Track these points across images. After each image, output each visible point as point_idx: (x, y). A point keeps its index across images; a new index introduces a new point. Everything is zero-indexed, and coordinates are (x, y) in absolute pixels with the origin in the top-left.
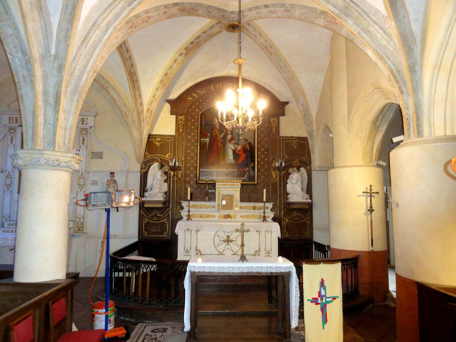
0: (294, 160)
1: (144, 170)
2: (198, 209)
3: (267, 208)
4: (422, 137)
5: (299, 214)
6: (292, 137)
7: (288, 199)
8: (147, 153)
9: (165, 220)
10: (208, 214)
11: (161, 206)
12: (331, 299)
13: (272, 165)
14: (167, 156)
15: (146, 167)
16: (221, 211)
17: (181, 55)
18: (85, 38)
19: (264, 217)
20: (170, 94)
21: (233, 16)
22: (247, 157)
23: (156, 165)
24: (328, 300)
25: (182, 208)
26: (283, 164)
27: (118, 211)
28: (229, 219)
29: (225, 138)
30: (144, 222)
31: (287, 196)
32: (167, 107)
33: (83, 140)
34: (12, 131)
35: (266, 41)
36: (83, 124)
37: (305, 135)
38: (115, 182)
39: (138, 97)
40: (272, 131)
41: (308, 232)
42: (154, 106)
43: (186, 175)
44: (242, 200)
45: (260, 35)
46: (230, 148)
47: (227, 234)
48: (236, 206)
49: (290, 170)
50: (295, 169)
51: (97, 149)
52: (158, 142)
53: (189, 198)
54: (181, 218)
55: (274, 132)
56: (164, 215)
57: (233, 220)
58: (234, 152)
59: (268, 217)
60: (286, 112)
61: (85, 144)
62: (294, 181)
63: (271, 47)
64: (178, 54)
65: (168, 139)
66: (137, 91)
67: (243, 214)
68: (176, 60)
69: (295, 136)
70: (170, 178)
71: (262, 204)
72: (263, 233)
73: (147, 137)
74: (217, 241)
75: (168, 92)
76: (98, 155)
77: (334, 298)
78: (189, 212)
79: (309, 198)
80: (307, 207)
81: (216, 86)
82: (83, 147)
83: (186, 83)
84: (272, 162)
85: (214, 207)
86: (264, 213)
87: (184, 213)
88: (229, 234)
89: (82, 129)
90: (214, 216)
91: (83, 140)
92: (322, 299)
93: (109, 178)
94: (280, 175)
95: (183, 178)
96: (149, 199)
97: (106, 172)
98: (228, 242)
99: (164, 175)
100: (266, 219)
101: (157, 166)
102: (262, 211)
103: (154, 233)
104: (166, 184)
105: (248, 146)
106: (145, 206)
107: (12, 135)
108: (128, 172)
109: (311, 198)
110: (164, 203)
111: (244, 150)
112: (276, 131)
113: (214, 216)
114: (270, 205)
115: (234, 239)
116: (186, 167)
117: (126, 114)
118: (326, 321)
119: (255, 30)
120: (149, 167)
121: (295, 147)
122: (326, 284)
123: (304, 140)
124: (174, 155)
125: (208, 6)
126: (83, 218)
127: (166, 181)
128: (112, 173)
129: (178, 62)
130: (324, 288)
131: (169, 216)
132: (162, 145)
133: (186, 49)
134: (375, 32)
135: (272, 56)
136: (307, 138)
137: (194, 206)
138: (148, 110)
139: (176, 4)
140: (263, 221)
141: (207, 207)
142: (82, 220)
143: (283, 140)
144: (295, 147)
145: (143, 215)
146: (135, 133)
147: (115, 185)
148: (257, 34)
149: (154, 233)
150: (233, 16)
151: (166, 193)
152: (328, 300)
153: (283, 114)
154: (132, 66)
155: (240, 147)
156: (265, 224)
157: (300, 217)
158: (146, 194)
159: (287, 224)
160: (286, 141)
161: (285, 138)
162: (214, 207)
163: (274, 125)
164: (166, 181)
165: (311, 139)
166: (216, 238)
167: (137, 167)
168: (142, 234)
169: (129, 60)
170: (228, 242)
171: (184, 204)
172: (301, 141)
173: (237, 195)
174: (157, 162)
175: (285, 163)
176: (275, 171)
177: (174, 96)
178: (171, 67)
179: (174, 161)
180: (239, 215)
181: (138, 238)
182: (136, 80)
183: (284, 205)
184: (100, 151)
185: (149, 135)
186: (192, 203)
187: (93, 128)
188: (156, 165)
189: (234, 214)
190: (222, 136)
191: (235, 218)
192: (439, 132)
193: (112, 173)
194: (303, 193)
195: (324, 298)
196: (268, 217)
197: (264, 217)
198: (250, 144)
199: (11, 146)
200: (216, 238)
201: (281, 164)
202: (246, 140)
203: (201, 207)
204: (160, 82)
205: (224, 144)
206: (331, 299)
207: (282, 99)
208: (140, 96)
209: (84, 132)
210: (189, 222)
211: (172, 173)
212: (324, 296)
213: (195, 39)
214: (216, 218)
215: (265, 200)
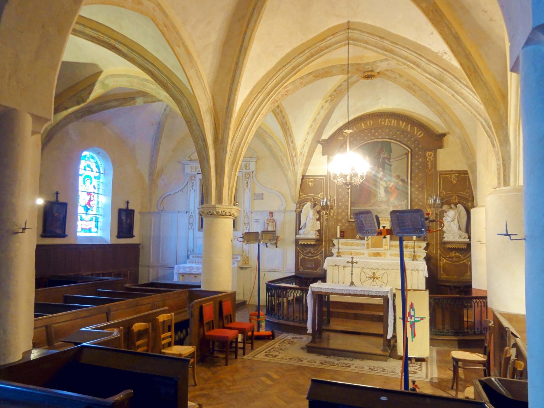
0: (453, 196)
1: (299, 210)
2: (349, 247)
3: (420, 247)
4: (509, 185)
5: (457, 254)
6: (452, 171)
7: (444, 238)
8: (301, 193)
9: (319, 256)
10: (358, 251)
11: (313, 243)
12: (419, 319)
13: (427, 202)
14: (319, 196)
15: (300, 206)
16: (371, 248)
17: (326, 102)
18: (240, 124)
19: (414, 256)
20: (322, 135)
21: (367, 67)
23: (309, 204)
24: (416, 319)
25: (334, 245)
26: (438, 201)
27: (277, 247)
28: (379, 257)
30: (300, 258)
31: (443, 235)
32: (320, 147)
33: (247, 183)
34: (193, 178)
35: (408, 80)
36: (246, 169)
37: (465, 168)
38: (274, 221)
40: (427, 165)
41: (469, 273)
42: (306, 150)
43: (338, 214)
45: (401, 76)
46: (382, 185)
47: (373, 271)
48: (386, 245)
49: (445, 207)
50: (452, 206)
51: (258, 191)
52: (312, 182)
53: (338, 236)
54: (332, 255)
55: (430, 166)
56: (317, 252)
57: (382, 258)
59: (420, 256)
60: (445, 144)
61: (249, 186)
62: (449, 219)
63: (414, 84)
64: (324, 101)
65: (321, 179)
66: (289, 138)
67: (393, 253)
68: (322, 107)
69: (455, 169)
70: (323, 216)
73: (301, 178)
75: (321, 134)
76: (261, 197)
77: (422, 319)
78: (339, 249)
79: (467, 237)
80: (465, 247)
81: (366, 123)
82: (247, 190)
83: (337, 123)
84: (427, 199)
85: (364, 245)
86: (414, 252)
87: (334, 251)
88: (375, 271)
89: (246, 174)
90: (363, 254)
91: (247, 183)
92: (411, 319)
93: (269, 217)
94: (436, 214)
95: (335, 217)
97: (266, 211)
98: (374, 279)
99: (316, 214)
100: (417, 258)
101: (309, 206)
102: (413, 250)
103: (308, 268)
104: (319, 222)
106: (300, 243)
107: (193, 181)
108: (285, 211)
109: (469, 238)
110: (317, 240)
112: (432, 165)
113: (363, 254)
114: (424, 244)
115: (380, 276)
116: (338, 205)
117: (282, 159)
118: (415, 336)
119: (394, 72)
120: (303, 205)
121: (454, 182)
122: (414, 307)
123: (464, 174)
124: (326, 194)
125: (341, 65)
126: (248, 252)
127: (318, 220)
128: (271, 213)
129: (324, 108)
130: (414, 310)
131: (322, 252)
132: (314, 185)
133: (331, 96)
134: (467, 94)
135: (416, 93)
136: (466, 171)
137: (342, 244)
138: (301, 153)
139: (311, 73)
140: (413, 260)
141: (358, 245)
142: (248, 255)
143: (440, 175)
144: (454, 182)
145: (299, 252)
146: (290, 174)
147: (274, 223)
148: (397, 76)
149: (308, 268)
150: (367, 67)
151: (319, 231)
152: (416, 319)
153: (441, 147)
154: (284, 117)
156: (415, 262)
157: (459, 258)
158: (301, 232)
159: (443, 265)
160: (444, 176)
161: (442, 173)
162: (364, 245)
163: (430, 159)
164: (318, 220)
165: (472, 172)
166: (362, 274)
167: (293, 206)
168: (298, 269)
169: (280, 113)
170: (374, 279)
171: (335, 241)
172: (461, 175)
174: (311, 201)
175: (441, 200)
176: (430, 208)
177: (326, 136)
178: (318, 114)
179: (325, 200)
182: (288, 129)
183: (441, 244)
184: (261, 193)
185: (303, 177)
186: (342, 241)
187: (254, 173)
188: (309, 204)
189: (383, 252)
191: (385, 256)
194: (460, 232)
195: (413, 318)
196: (420, 256)
197: (414, 256)
199: (192, 191)
200: (363, 274)
201: (435, 201)
203: (352, 245)
204: (310, 127)
206: (419, 319)
207: (441, 131)
208: (292, 142)
210: (339, 258)
211: (324, 212)
212: (414, 316)
213: (338, 87)
214: (366, 255)
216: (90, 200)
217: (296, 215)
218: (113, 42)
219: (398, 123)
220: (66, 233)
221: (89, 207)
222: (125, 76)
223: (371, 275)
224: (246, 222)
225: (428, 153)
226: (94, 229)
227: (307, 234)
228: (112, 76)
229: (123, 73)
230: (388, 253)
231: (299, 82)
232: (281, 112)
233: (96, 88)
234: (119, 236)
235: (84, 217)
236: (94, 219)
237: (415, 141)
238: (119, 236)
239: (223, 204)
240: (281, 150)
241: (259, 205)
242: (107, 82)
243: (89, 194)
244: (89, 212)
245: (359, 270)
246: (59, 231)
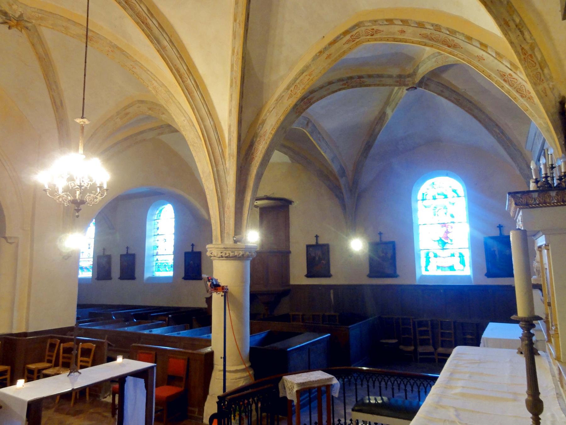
39: (481, 53)
154: (421, 25)
169: (405, 28)
182: (453, 32)
216: (447, 232)
220: (398, 272)
221: (446, 241)
226: (458, 266)
231: (238, 25)
232: (405, 22)
234: (489, 275)
235: (440, 253)
236: (457, 255)
238: (489, 275)
239: (214, 242)
243: (444, 225)
244: (447, 246)
246: (389, 271)
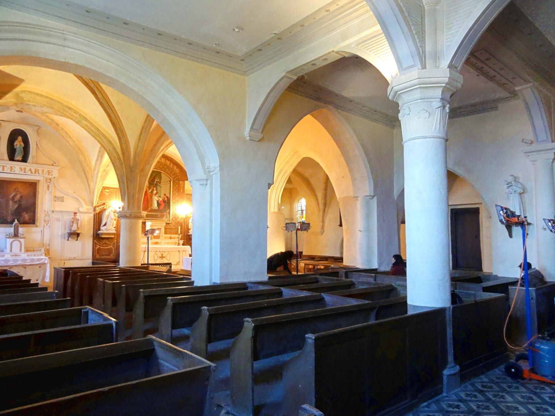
22: (165, 206)
29: (152, 192)
33: (48, 187)
36: (49, 174)
44: (166, 233)
51: (58, 194)
58: (158, 202)
61: (50, 190)
71: (177, 236)
72: (181, 252)
74: (156, 256)
76: (62, 199)
91: (48, 187)
96: (105, 232)
105: (166, 199)
111: (164, 201)
126: (49, 245)
128: (75, 213)
138: (105, 170)
145: (96, 243)
146: (92, 184)
155: (161, 199)
166: (156, 256)
173: (163, 230)
180: (163, 242)
181: (93, 259)
190: (150, 191)
192: (272, 210)
193: (75, 213)
198: (167, 197)
200: (156, 256)
202: (165, 195)
205: (151, 197)
209: (49, 181)
215: (179, 233)
217: (94, 215)
218: (95, 89)
219: (165, 161)
222: (47, 97)
223: (160, 255)
224: (46, 219)
225: (181, 182)
227: (109, 230)
228: (31, 92)
229: (45, 94)
230: (163, 242)
233: (7, 96)
237: (174, 174)
240: (88, 165)
241: (58, 206)
242: (23, 95)
245: (154, 253)
